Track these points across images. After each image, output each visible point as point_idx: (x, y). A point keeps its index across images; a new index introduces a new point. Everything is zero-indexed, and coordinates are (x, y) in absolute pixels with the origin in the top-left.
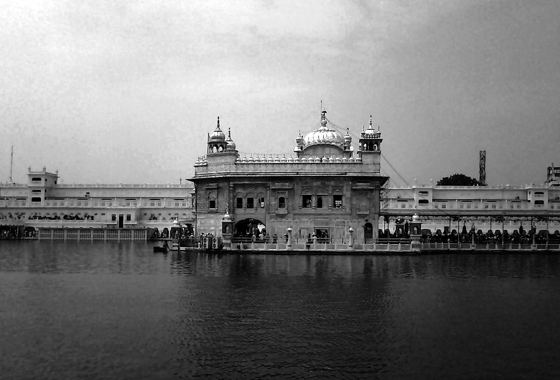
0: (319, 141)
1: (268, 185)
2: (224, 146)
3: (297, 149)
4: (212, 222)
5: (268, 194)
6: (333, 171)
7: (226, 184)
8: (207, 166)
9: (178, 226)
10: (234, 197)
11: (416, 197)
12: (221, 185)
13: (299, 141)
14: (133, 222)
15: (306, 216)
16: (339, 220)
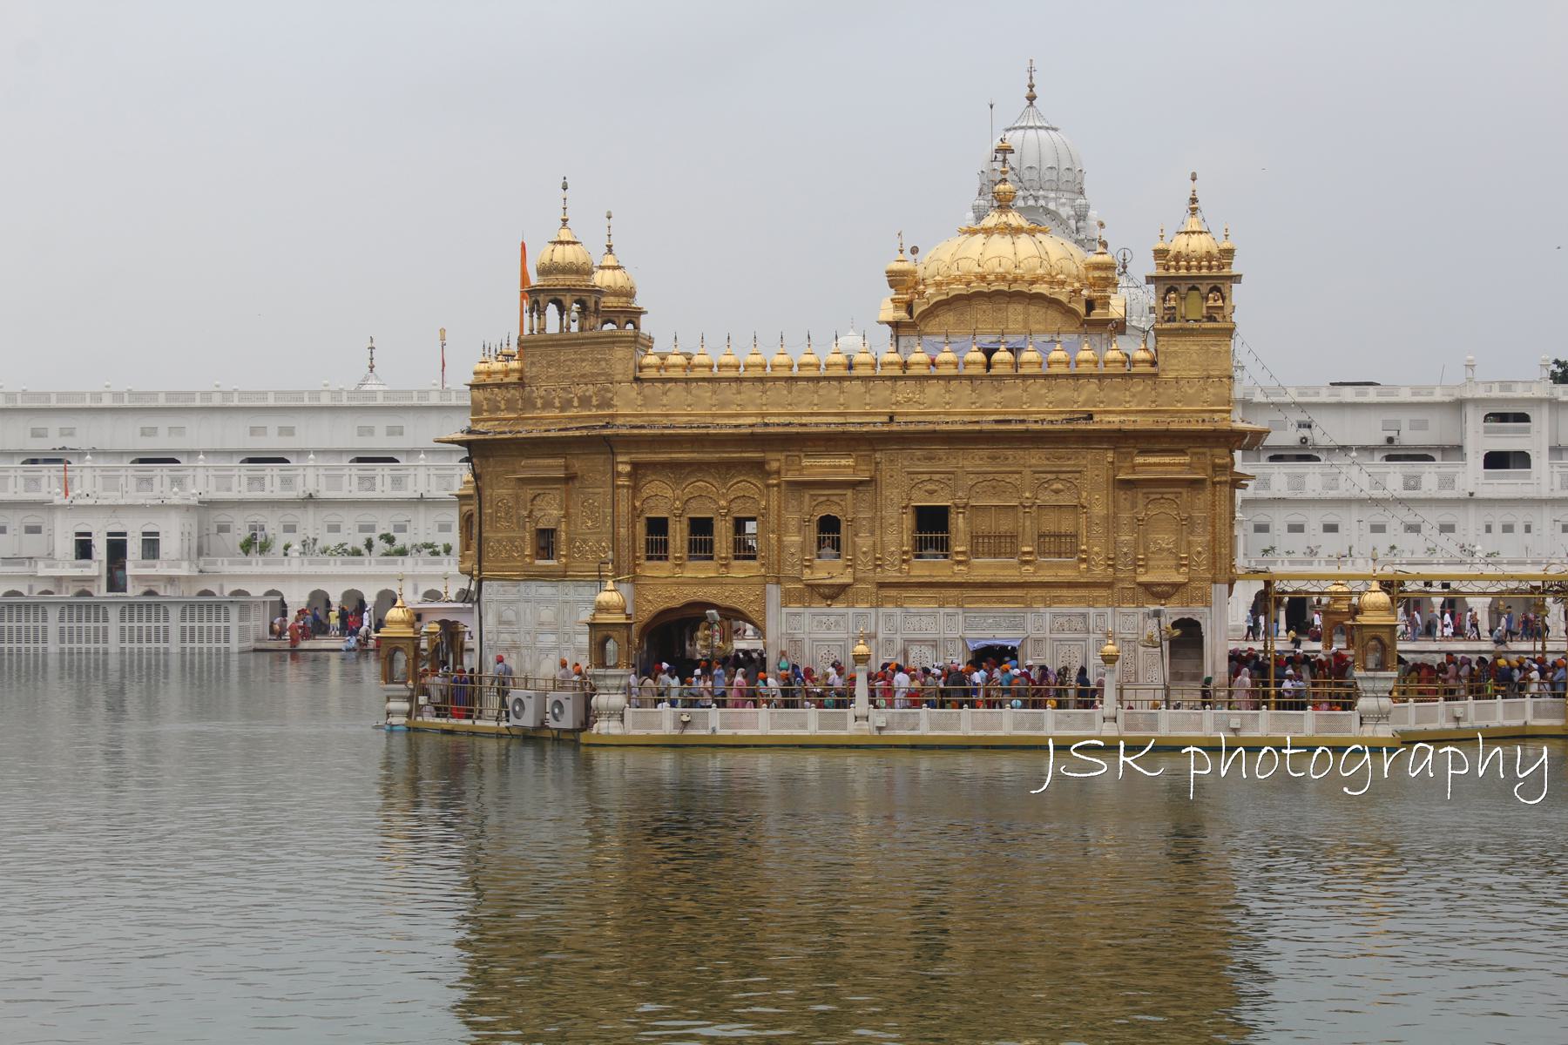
0: (983, 278)
1: (774, 465)
2: (591, 304)
3: (889, 312)
4: (547, 614)
5: (774, 504)
6: (1043, 408)
7: (599, 460)
8: (521, 383)
9: (409, 633)
10: (635, 513)
11: (1480, 439)
12: (577, 465)
13: (897, 280)
14: (174, 560)
15: (929, 593)
16: (1065, 608)
